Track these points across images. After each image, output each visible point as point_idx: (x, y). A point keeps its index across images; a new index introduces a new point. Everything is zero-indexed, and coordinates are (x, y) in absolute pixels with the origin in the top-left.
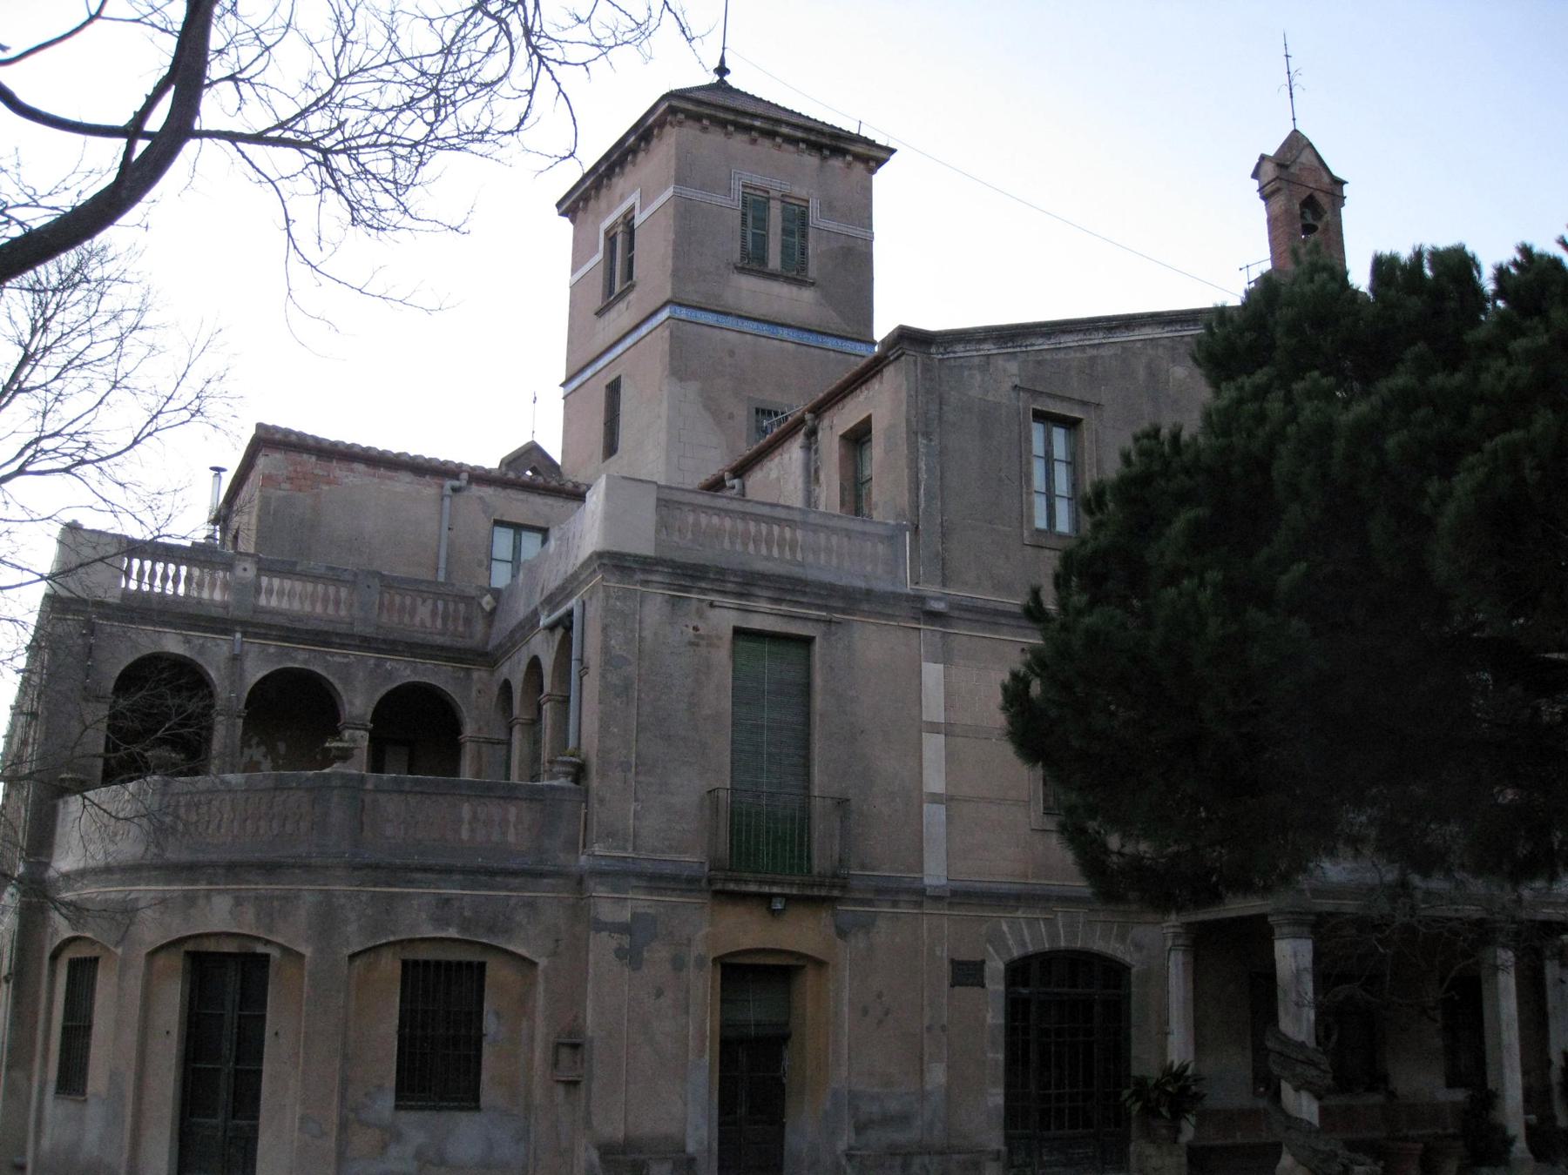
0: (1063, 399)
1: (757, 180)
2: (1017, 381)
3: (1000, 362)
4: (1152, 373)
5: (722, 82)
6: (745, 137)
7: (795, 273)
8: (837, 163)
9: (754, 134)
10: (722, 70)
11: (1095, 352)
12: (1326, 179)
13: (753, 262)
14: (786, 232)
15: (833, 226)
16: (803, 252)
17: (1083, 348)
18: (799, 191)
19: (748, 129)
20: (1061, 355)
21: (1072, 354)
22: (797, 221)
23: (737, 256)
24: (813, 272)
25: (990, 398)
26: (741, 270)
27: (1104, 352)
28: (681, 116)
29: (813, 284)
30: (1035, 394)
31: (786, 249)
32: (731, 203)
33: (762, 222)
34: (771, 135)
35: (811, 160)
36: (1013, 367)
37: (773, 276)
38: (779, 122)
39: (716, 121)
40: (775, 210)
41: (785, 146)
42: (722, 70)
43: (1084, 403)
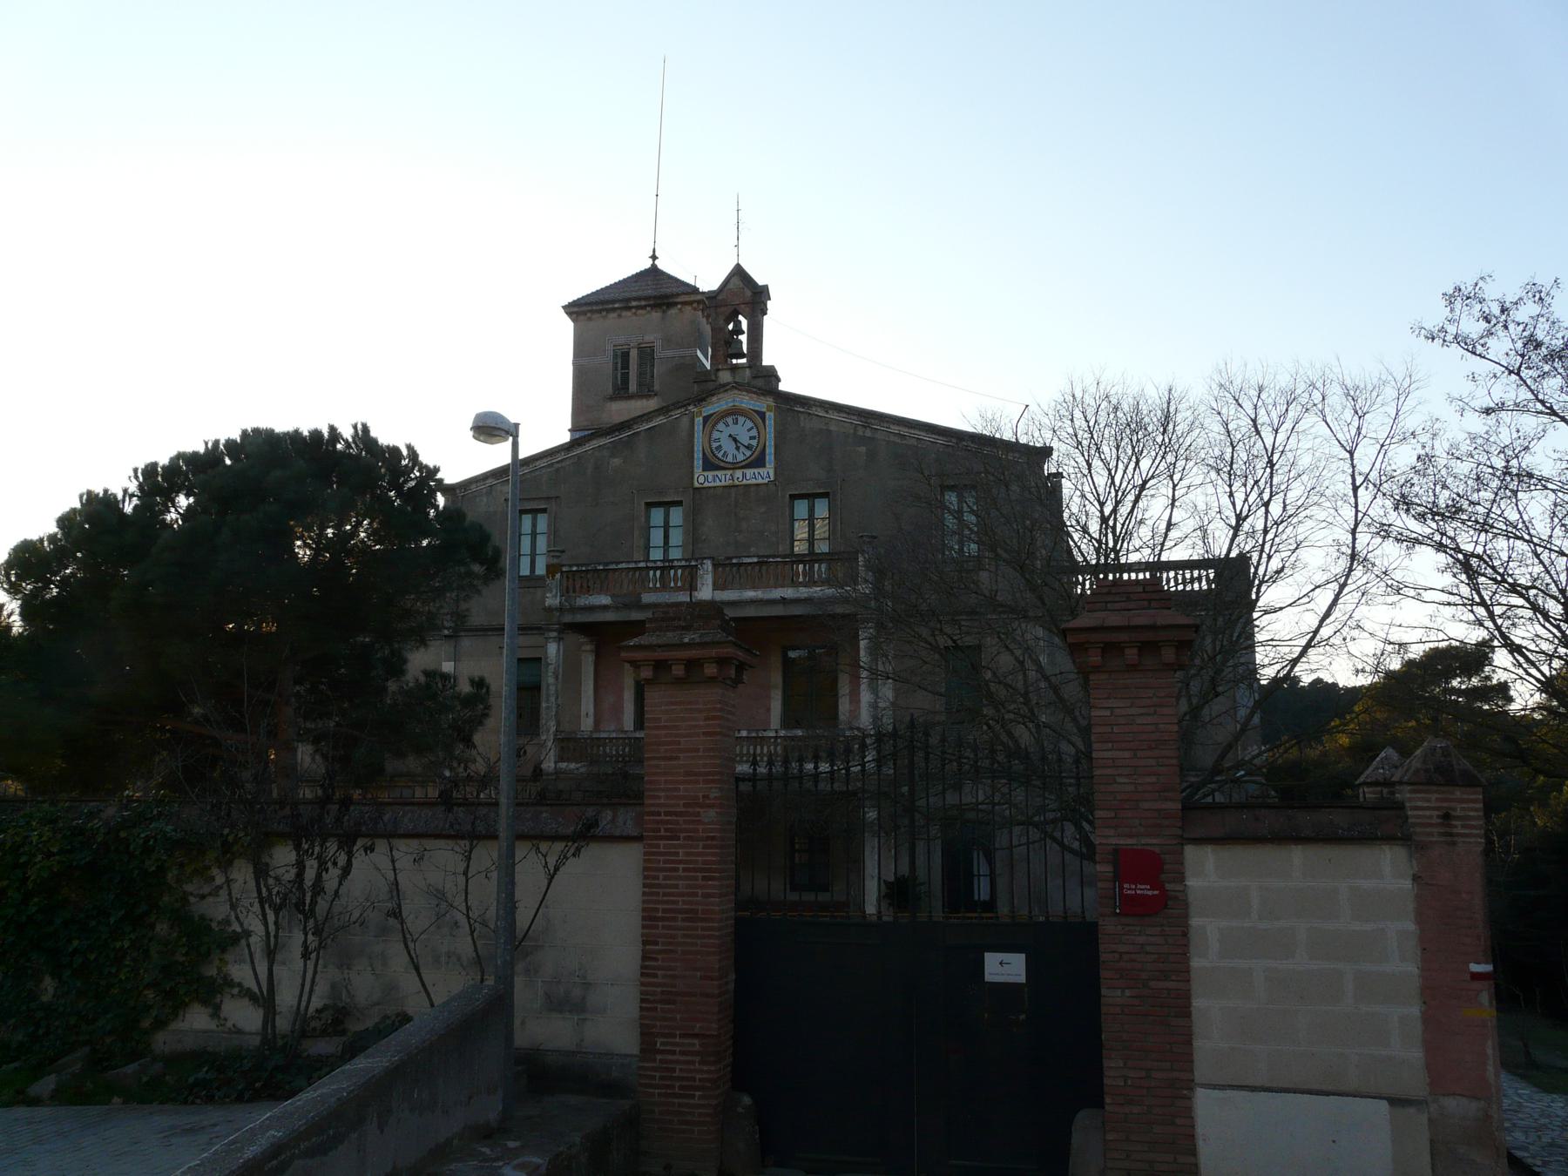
1: (622, 340)
3: (499, 487)
5: (654, 266)
6: (614, 315)
7: (646, 391)
8: (673, 311)
10: (654, 257)
12: (748, 293)
13: (621, 391)
14: (640, 365)
15: (669, 353)
18: (648, 338)
19: (614, 310)
22: (647, 354)
23: (610, 391)
24: (656, 387)
26: (612, 398)
31: (641, 375)
32: (605, 362)
33: (626, 365)
34: (630, 308)
35: (656, 315)
37: (631, 397)
38: (629, 300)
39: (592, 311)
40: (634, 354)
42: (654, 257)
43: (548, 499)
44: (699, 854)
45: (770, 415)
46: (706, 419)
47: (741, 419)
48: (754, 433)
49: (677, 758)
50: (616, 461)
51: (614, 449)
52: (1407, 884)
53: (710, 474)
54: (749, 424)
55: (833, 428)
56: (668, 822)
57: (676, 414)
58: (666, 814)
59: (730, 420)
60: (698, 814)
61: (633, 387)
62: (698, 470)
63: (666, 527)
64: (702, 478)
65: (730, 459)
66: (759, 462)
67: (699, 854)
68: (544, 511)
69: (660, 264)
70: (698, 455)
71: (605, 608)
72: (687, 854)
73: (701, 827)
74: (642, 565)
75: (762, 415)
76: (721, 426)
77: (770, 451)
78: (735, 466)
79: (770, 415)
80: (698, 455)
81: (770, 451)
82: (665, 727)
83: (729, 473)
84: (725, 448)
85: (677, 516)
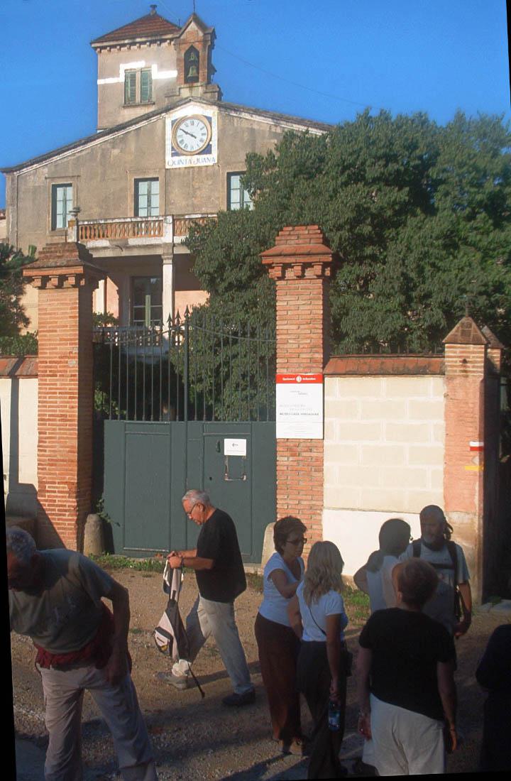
0: (63, 177)
2: (47, 175)
4: (103, 156)
9: (128, 46)
11: (78, 155)
16: (151, 89)
17: (74, 154)
20: (65, 160)
21: (70, 158)
24: (154, 99)
25: (37, 185)
27: (84, 153)
28: (99, 50)
29: (154, 104)
30: (53, 178)
36: (46, 170)
40: (138, 76)
41: (142, 46)
44: (68, 384)
45: (215, 121)
46: (173, 122)
47: (196, 122)
48: (205, 131)
49: (56, 331)
50: (116, 152)
51: (114, 144)
52: (442, 399)
53: (176, 159)
54: (201, 125)
55: (256, 127)
56: (51, 367)
57: (154, 119)
58: (50, 362)
59: (188, 122)
60: (67, 362)
61: (138, 99)
62: (168, 158)
63: (149, 195)
64: (171, 162)
65: (189, 149)
66: (207, 150)
67: (68, 384)
68: (70, 185)
69: (159, 11)
70: (168, 148)
71: (105, 248)
72: (62, 385)
73: (68, 369)
74: (134, 220)
75: (209, 119)
76: (183, 126)
77: (214, 143)
78: (192, 154)
79: (215, 121)
80: (168, 148)
81: (214, 143)
82: (50, 314)
83: (189, 157)
84: (185, 142)
85: (156, 187)
